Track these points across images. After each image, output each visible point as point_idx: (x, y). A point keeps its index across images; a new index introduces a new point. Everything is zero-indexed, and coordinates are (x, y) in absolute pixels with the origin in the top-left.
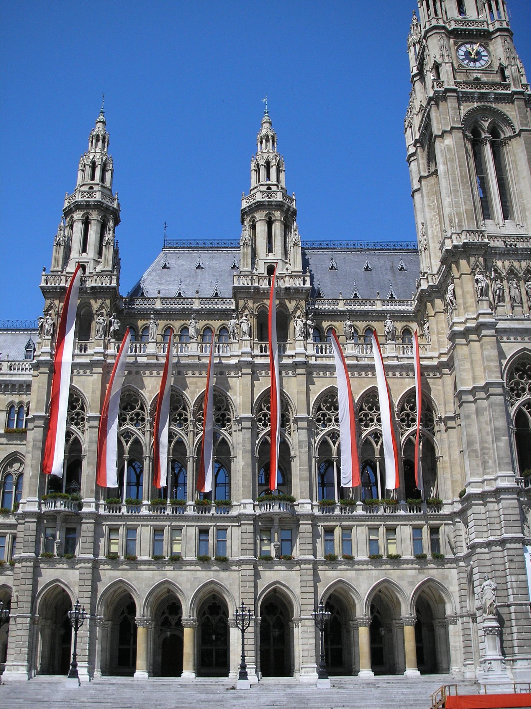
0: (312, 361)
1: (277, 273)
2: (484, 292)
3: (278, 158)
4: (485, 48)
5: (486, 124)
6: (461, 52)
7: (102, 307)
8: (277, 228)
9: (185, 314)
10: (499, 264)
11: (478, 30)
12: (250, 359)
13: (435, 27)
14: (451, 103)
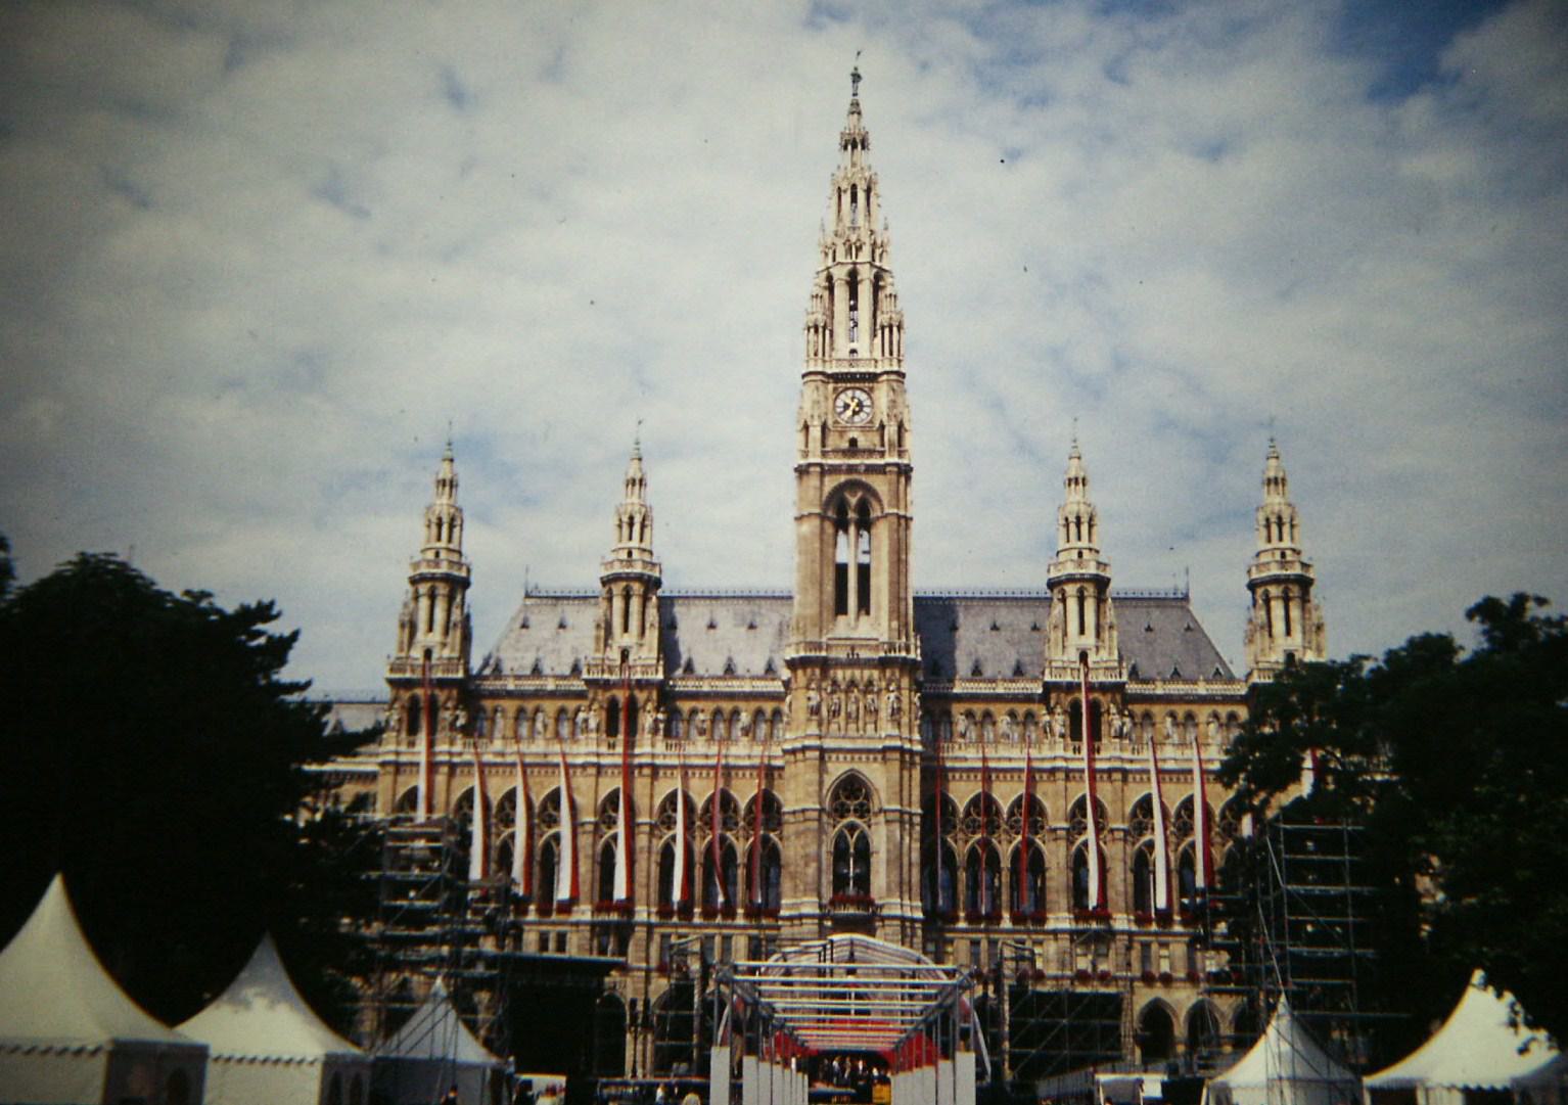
0: (659, 761)
1: (631, 657)
3: (643, 510)
4: (868, 394)
5: (853, 501)
6: (840, 403)
7: (448, 699)
8: (635, 603)
9: (539, 694)
10: (840, 674)
11: (861, 374)
12: (594, 759)
13: (810, 373)
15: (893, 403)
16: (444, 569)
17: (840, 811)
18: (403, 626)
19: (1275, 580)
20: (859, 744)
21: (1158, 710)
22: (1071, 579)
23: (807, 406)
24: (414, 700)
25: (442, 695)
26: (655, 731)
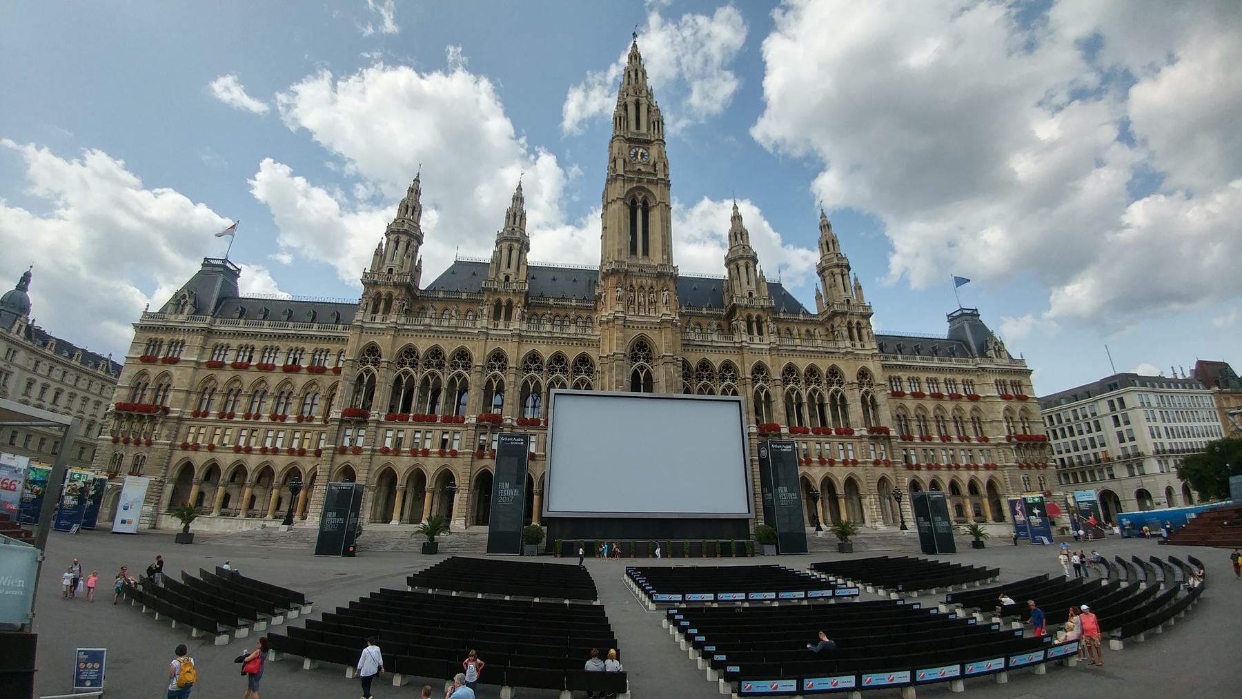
2: (620, 299)
8: (515, 254)
14: (619, 183)
15: (660, 152)
16: (406, 227)
17: (635, 358)
18: (376, 254)
19: (838, 266)
20: (646, 319)
21: (783, 327)
22: (741, 258)
23: (615, 151)
24: (379, 294)
25: (395, 293)
26: (523, 318)
